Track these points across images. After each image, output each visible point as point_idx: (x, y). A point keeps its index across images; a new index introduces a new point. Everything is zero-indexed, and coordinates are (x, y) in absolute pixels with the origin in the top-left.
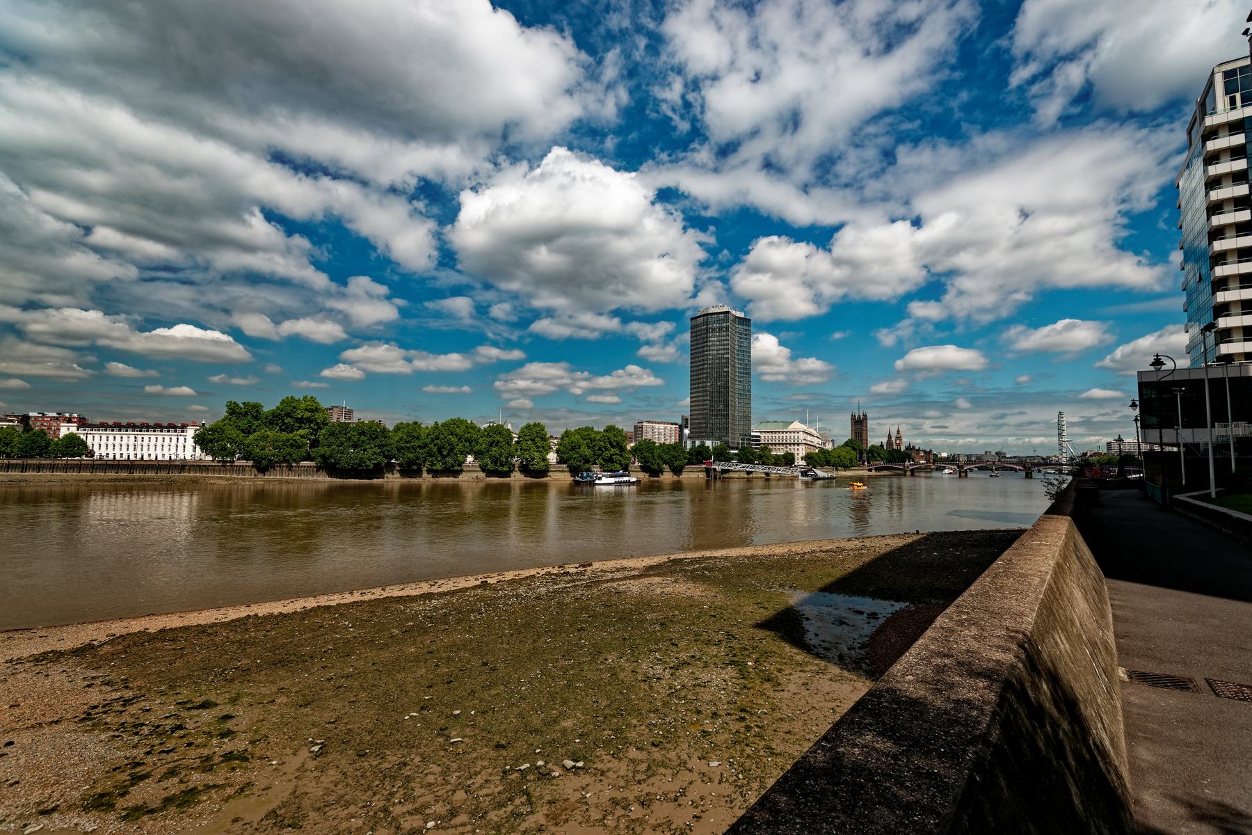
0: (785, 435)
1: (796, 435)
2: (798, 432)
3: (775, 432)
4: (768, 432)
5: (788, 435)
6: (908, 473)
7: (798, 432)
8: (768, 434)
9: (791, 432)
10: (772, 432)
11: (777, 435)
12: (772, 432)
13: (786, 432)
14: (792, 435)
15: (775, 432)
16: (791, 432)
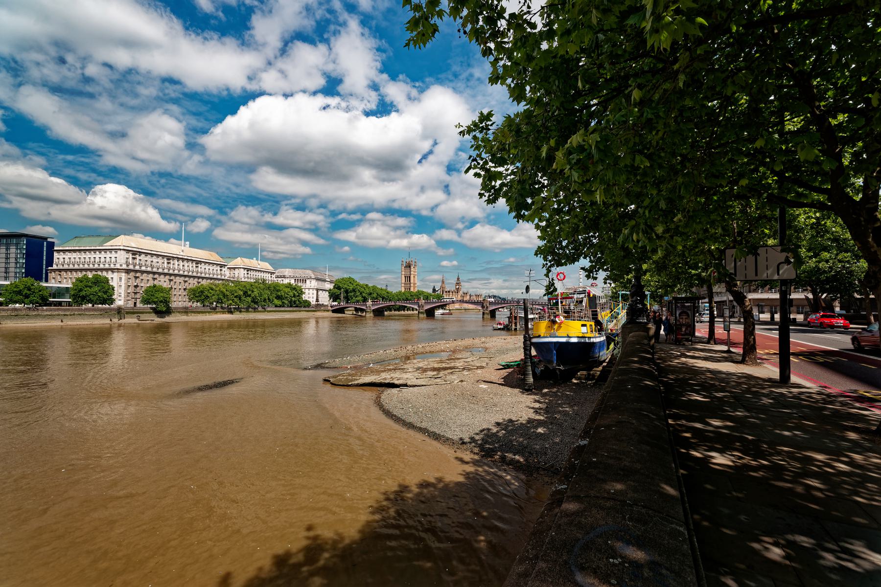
0: (98, 255)
1: (113, 255)
2: (116, 250)
3: (85, 251)
4: (75, 251)
5: (103, 255)
6: (370, 315)
7: (116, 250)
8: (74, 255)
9: (105, 250)
10: (80, 251)
11: (88, 255)
12: (80, 251)
13: (100, 251)
14: (108, 255)
15: (85, 251)
16: (105, 250)
